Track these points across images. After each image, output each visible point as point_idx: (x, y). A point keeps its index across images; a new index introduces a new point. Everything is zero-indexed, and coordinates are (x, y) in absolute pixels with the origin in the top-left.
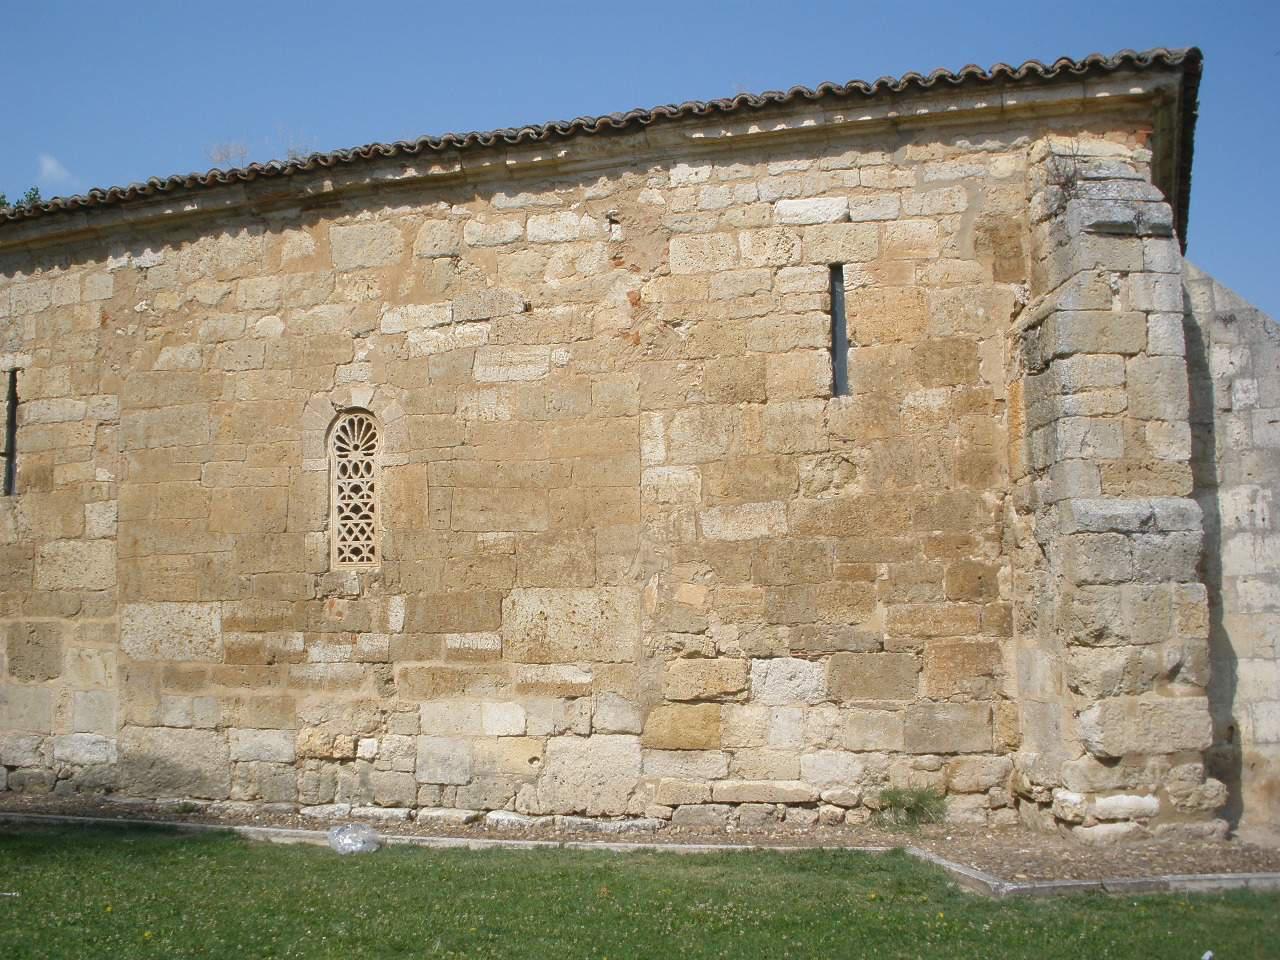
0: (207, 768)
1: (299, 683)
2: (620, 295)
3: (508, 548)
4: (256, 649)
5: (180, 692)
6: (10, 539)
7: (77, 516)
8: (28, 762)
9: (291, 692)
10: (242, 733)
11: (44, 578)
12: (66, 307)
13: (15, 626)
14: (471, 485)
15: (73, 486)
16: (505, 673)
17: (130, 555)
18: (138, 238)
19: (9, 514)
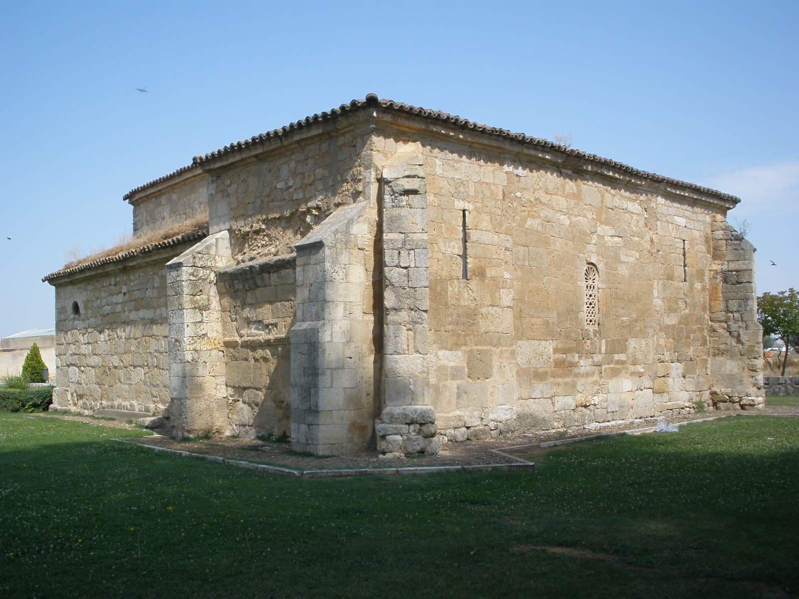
0: (546, 415)
1: (577, 375)
2: (647, 238)
3: (627, 323)
4: (564, 361)
5: (539, 382)
6: (466, 304)
7: (497, 294)
8: (476, 423)
9: (575, 379)
10: (560, 398)
11: (483, 326)
12: (487, 184)
13: (471, 351)
14: (620, 299)
15: (493, 279)
16: (627, 368)
17: (519, 316)
18: (519, 160)
19: (465, 290)
